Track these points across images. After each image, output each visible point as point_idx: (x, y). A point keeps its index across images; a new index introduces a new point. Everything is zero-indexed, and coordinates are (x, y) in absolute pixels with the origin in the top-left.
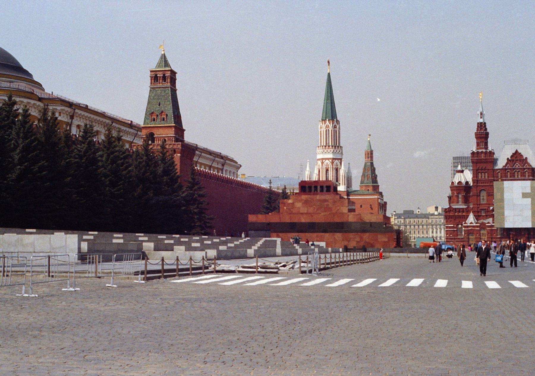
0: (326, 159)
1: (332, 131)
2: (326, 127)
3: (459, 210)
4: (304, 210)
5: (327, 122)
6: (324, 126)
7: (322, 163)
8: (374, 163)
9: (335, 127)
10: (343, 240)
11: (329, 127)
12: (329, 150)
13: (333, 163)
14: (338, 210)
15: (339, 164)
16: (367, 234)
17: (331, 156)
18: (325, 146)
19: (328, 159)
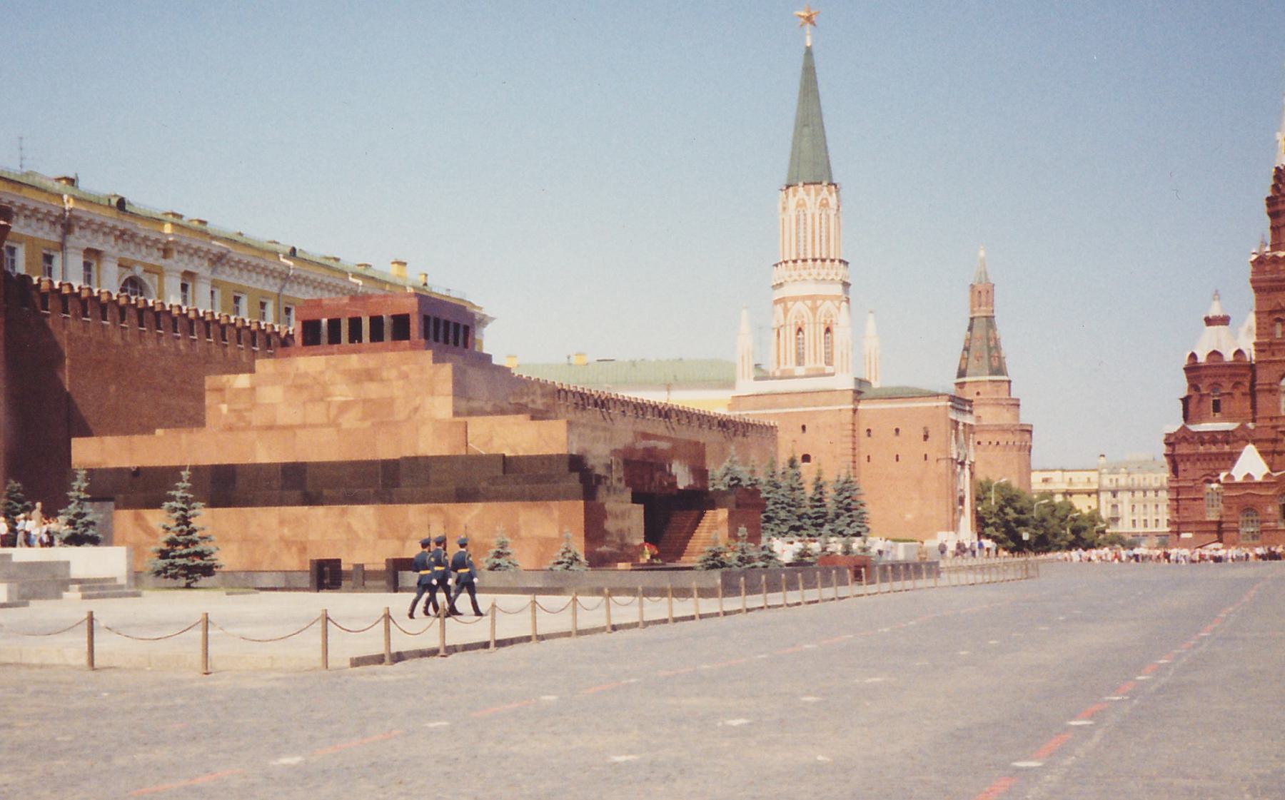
0: (795, 299)
1: (813, 216)
2: (798, 205)
3: (1213, 437)
4: (287, 415)
5: (801, 189)
6: (792, 202)
7: (786, 311)
8: (997, 320)
9: (825, 205)
10: (381, 536)
11: (805, 205)
12: (805, 273)
13: (814, 309)
14: (416, 409)
15: (834, 311)
16: (477, 509)
17: (810, 289)
18: (795, 261)
19: (804, 298)
